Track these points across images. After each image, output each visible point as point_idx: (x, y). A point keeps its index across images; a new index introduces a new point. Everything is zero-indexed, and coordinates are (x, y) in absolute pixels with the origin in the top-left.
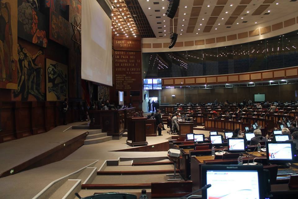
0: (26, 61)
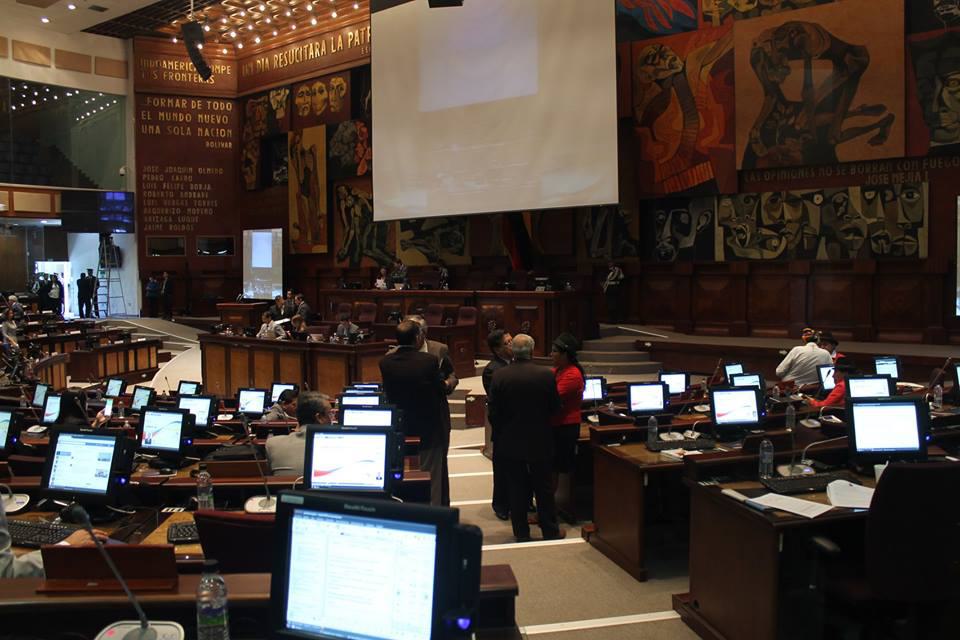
0: (356, 206)
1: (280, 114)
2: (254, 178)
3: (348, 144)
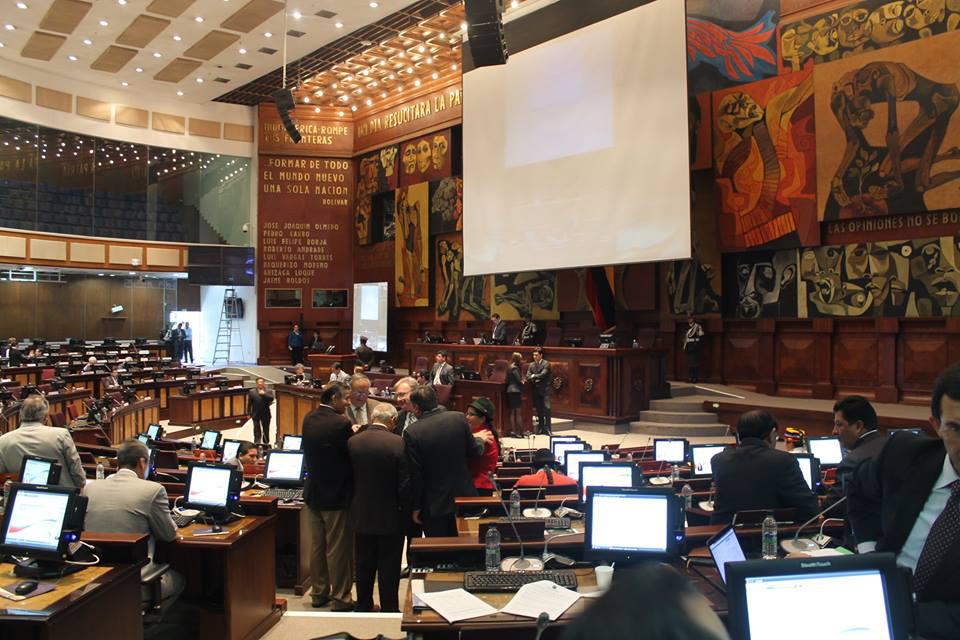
1: (389, 172)
2: (365, 234)
3: (448, 200)
